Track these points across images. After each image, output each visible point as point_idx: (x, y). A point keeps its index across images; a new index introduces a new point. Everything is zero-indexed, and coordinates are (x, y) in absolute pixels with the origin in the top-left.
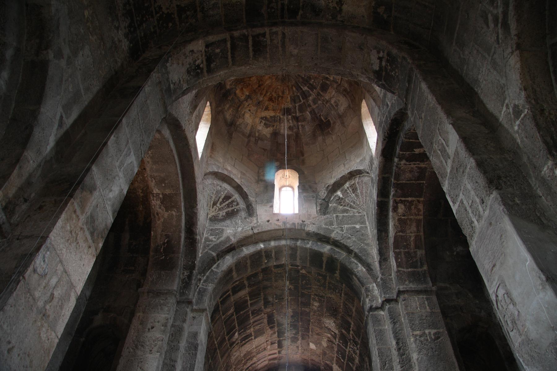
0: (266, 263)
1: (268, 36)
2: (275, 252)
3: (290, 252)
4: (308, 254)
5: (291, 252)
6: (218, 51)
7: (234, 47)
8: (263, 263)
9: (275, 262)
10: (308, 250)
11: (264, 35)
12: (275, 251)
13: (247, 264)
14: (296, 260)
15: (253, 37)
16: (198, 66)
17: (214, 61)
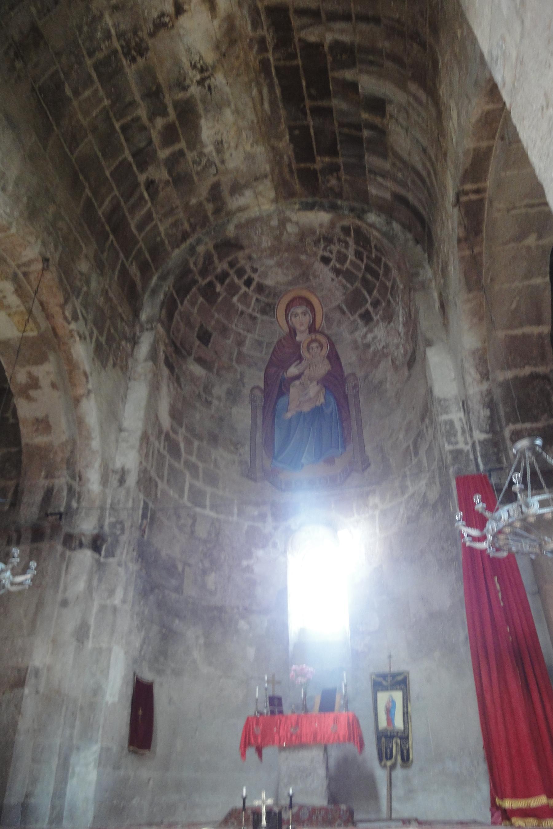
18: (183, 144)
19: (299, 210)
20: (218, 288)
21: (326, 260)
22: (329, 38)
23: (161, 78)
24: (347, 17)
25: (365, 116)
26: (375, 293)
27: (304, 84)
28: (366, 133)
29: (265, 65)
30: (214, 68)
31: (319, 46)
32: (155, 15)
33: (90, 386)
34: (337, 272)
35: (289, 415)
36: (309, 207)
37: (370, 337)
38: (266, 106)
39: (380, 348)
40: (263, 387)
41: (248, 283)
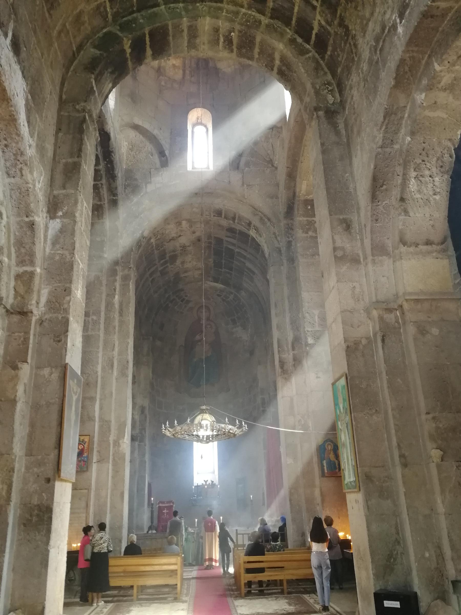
0: (234, 32)
1: (212, 216)
2: (218, 44)
3: (198, 41)
4: (171, 45)
5: (197, 41)
6: (243, 223)
7: (234, 219)
8: (237, 33)
9: (219, 27)
10: (172, 52)
11: (214, 216)
12: (219, 46)
13: (259, 54)
14: (190, 27)
15: (221, 217)
16: (255, 230)
17: (247, 223)
18: (168, 264)
19: (211, 282)
20: (170, 305)
21: (218, 295)
22: (237, 250)
23: (166, 251)
24: (246, 251)
25: (246, 270)
26: (239, 314)
27: (224, 254)
28: (245, 273)
29: (209, 247)
30: (189, 246)
31: (232, 250)
32: (170, 238)
33: (136, 380)
34: (224, 300)
35: (195, 360)
36: (216, 280)
37: (234, 330)
38: (206, 254)
39: (238, 337)
40: (184, 345)
41: (182, 301)
